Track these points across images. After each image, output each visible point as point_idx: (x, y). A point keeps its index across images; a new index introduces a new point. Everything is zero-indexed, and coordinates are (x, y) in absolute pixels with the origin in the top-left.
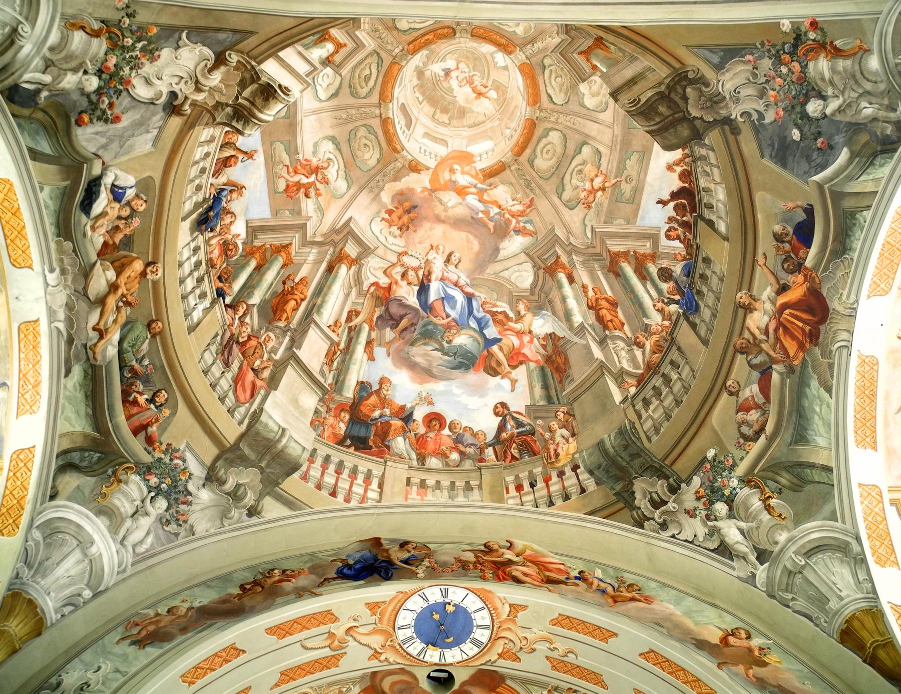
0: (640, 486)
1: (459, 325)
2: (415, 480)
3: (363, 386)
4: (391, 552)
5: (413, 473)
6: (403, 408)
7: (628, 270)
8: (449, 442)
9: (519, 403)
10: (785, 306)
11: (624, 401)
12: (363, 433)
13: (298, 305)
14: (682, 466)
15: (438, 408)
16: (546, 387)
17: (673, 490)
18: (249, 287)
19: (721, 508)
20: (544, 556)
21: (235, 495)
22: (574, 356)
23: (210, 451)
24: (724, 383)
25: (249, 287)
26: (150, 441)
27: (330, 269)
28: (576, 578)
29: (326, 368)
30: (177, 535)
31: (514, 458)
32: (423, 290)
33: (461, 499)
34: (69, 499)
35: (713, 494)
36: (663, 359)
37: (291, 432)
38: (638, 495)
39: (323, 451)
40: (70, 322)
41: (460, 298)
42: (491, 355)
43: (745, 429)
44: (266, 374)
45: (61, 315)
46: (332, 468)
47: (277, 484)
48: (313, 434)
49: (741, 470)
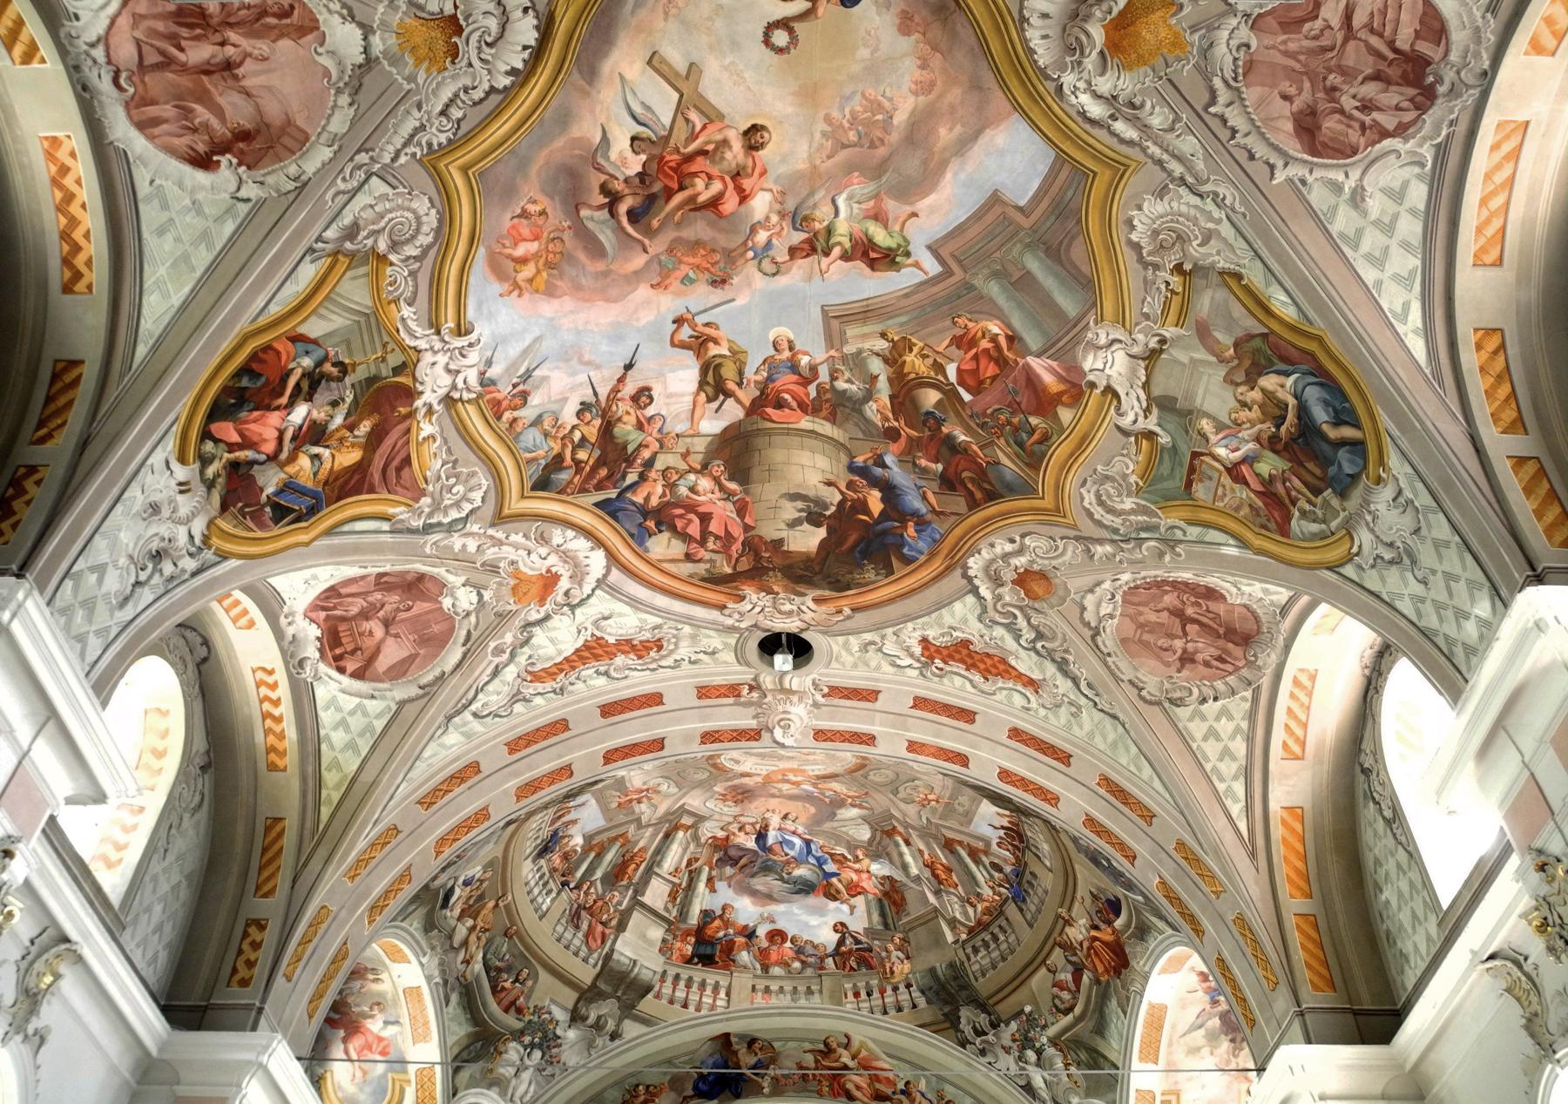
0: (965, 1013)
1: (798, 861)
2: (760, 987)
3: (707, 915)
4: (740, 1055)
5: (758, 981)
6: (746, 927)
7: (963, 853)
8: (791, 954)
9: (858, 924)
10: (1095, 939)
11: (956, 942)
12: (709, 951)
13: (638, 866)
14: (1004, 1009)
15: (781, 925)
16: (883, 915)
17: (994, 1026)
18: (591, 870)
19: (1031, 1055)
20: (878, 1059)
21: (598, 1026)
22: (910, 897)
23: (570, 996)
24: (1044, 961)
25: (591, 870)
26: (519, 1011)
27: (667, 836)
28: (902, 1092)
29: (670, 906)
30: (553, 1075)
31: (852, 968)
32: (761, 836)
33: (803, 1002)
34: (467, 1088)
35: (1026, 1042)
36: (992, 922)
37: (642, 961)
38: (963, 1021)
39: (672, 971)
40: (443, 972)
41: (797, 842)
42: (830, 885)
43: (1057, 1002)
44: (614, 923)
45: (436, 973)
46: (682, 984)
47: (633, 1007)
48: (662, 959)
49: (1052, 1031)
